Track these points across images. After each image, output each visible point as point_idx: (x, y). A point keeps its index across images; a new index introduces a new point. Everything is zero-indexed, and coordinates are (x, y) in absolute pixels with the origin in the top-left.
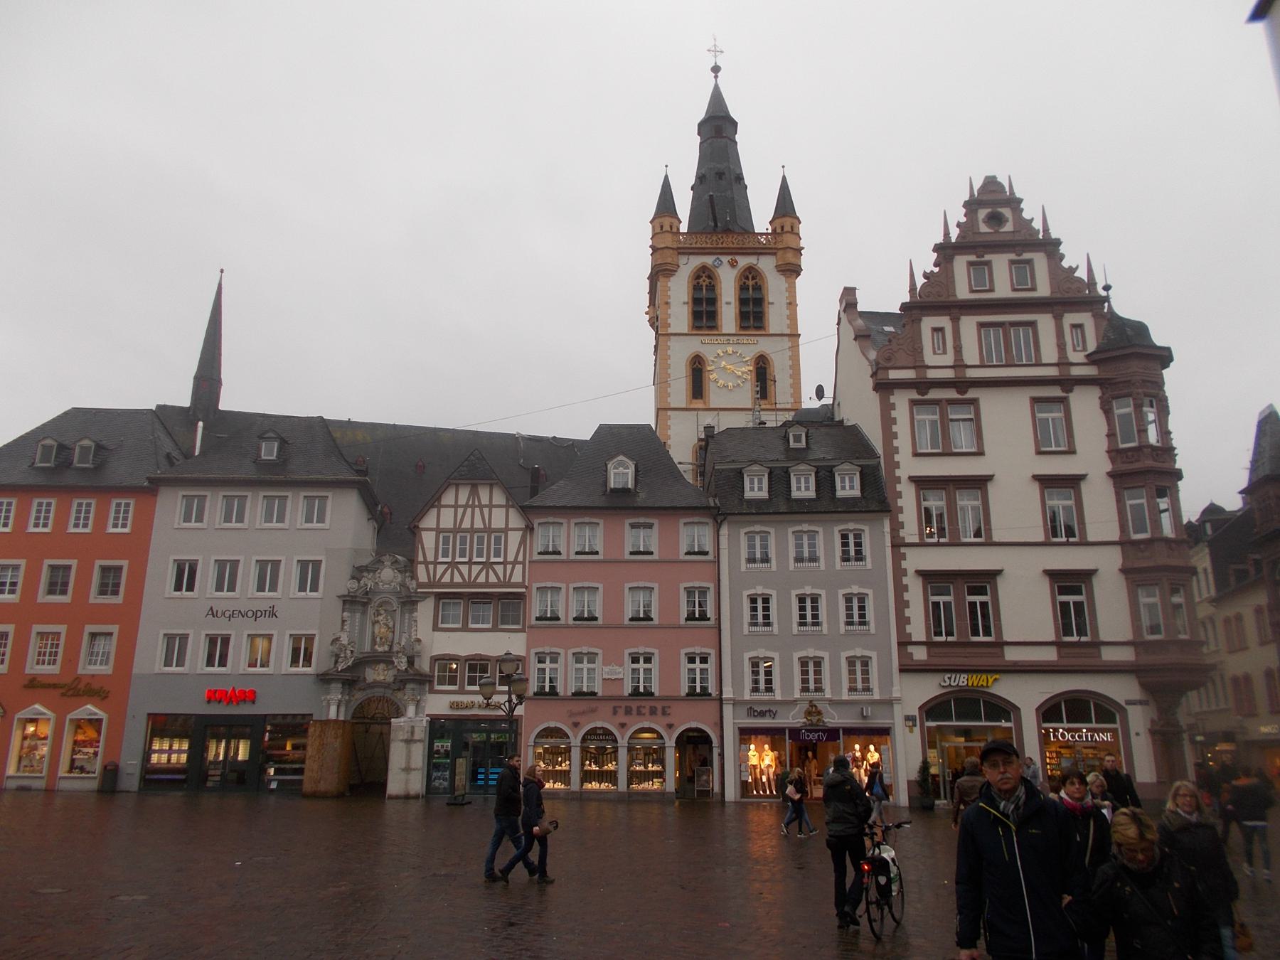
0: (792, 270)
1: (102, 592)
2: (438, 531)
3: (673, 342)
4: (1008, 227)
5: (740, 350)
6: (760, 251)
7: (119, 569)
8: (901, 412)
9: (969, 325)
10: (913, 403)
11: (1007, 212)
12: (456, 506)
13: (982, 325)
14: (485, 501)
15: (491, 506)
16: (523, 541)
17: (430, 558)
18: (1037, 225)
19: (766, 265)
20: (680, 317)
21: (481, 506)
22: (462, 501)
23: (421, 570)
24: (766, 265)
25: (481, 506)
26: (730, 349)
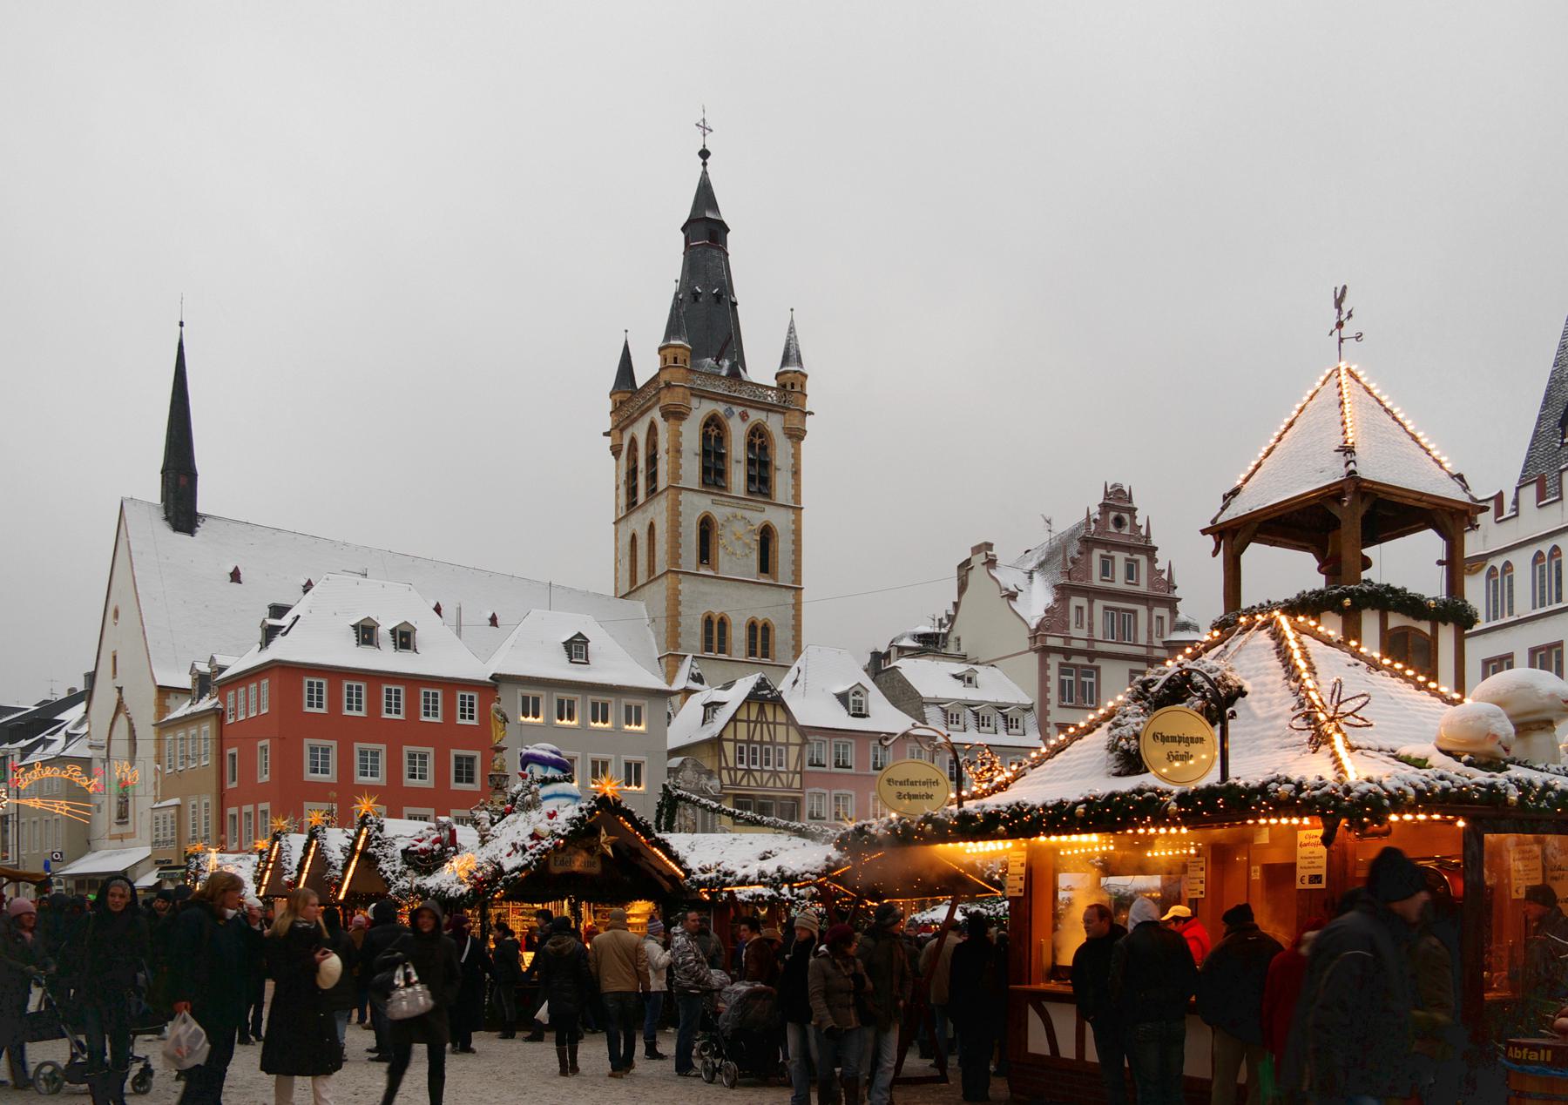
0: (796, 435)
1: (458, 780)
2: (736, 741)
3: (683, 496)
4: (1126, 531)
5: (748, 514)
6: (769, 408)
7: (471, 759)
8: (1053, 672)
9: (1099, 605)
10: (1061, 664)
11: (1126, 516)
12: (748, 721)
13: (1106, 608)
14: (770, 719)
15: (775, 723)
16: (800, 755)
17: (731, 765)
18: (1143, 531)
19: (774, 424)
20: (692, 468)
21: (768, 723)
22: (753, 718)
23: (724, 772)
24: (774, 424)
25: (768, 723)
26: (740, 513)
